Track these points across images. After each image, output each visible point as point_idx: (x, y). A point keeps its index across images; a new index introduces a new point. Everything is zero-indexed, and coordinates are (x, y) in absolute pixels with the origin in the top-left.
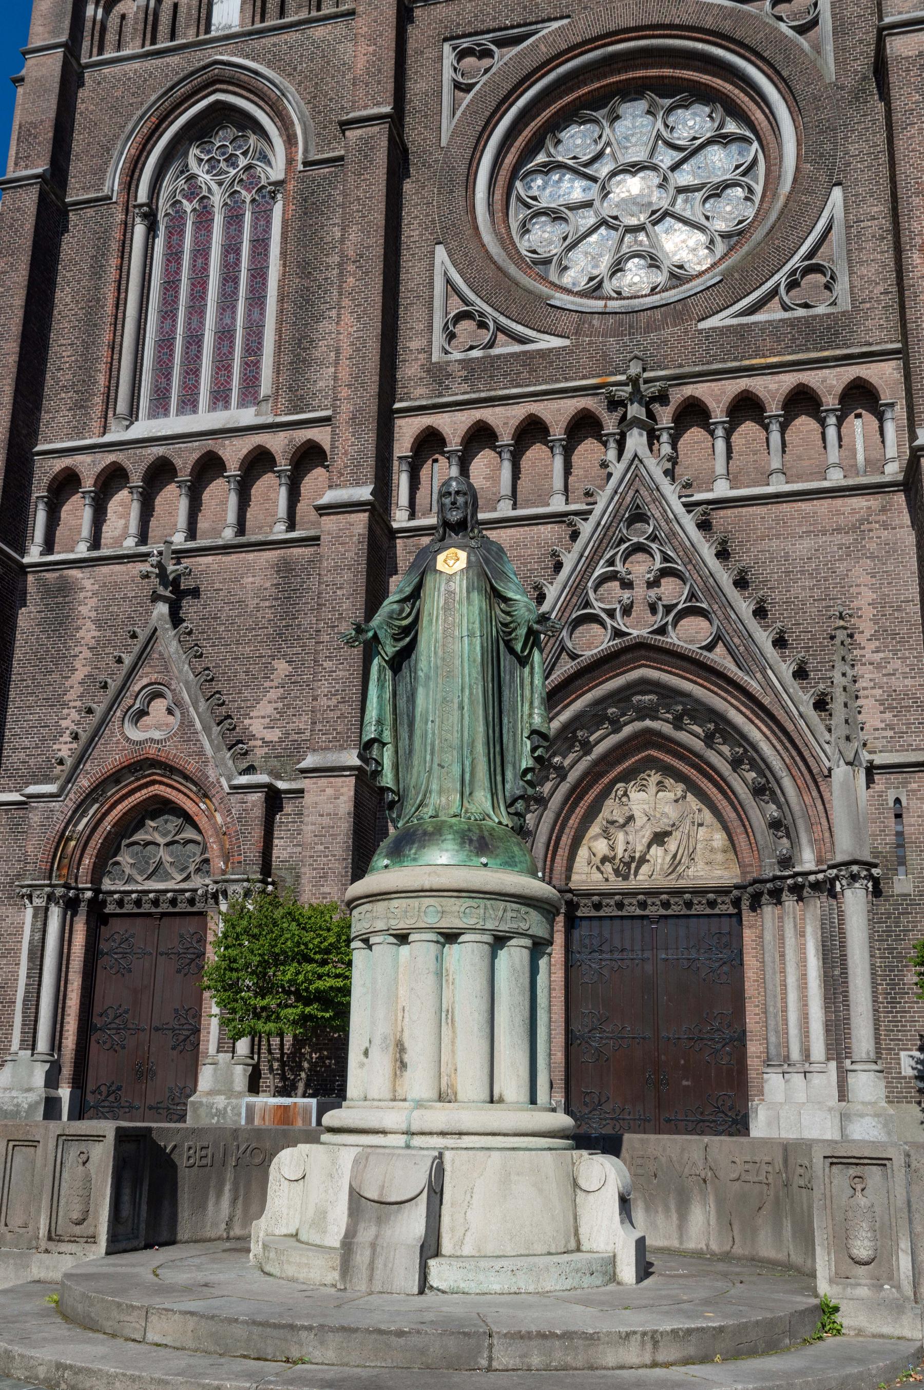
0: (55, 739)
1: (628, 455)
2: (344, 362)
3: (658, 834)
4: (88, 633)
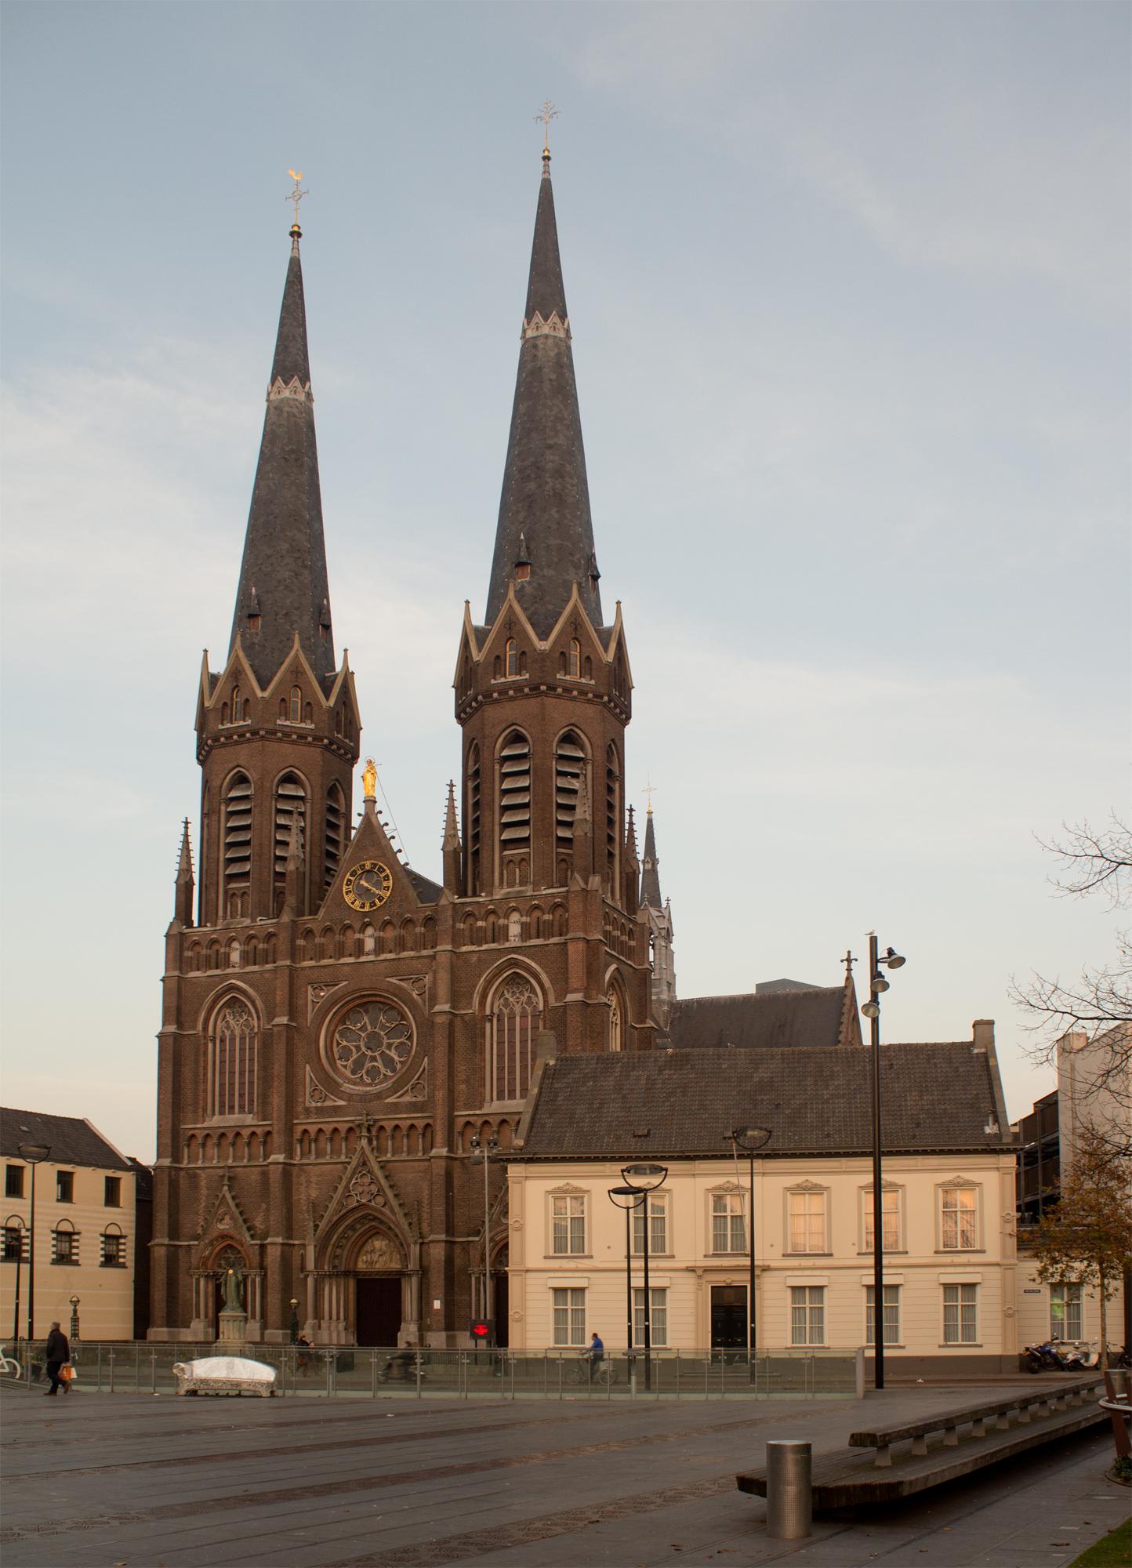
3: (378, 1257)
4: (204, 1191)
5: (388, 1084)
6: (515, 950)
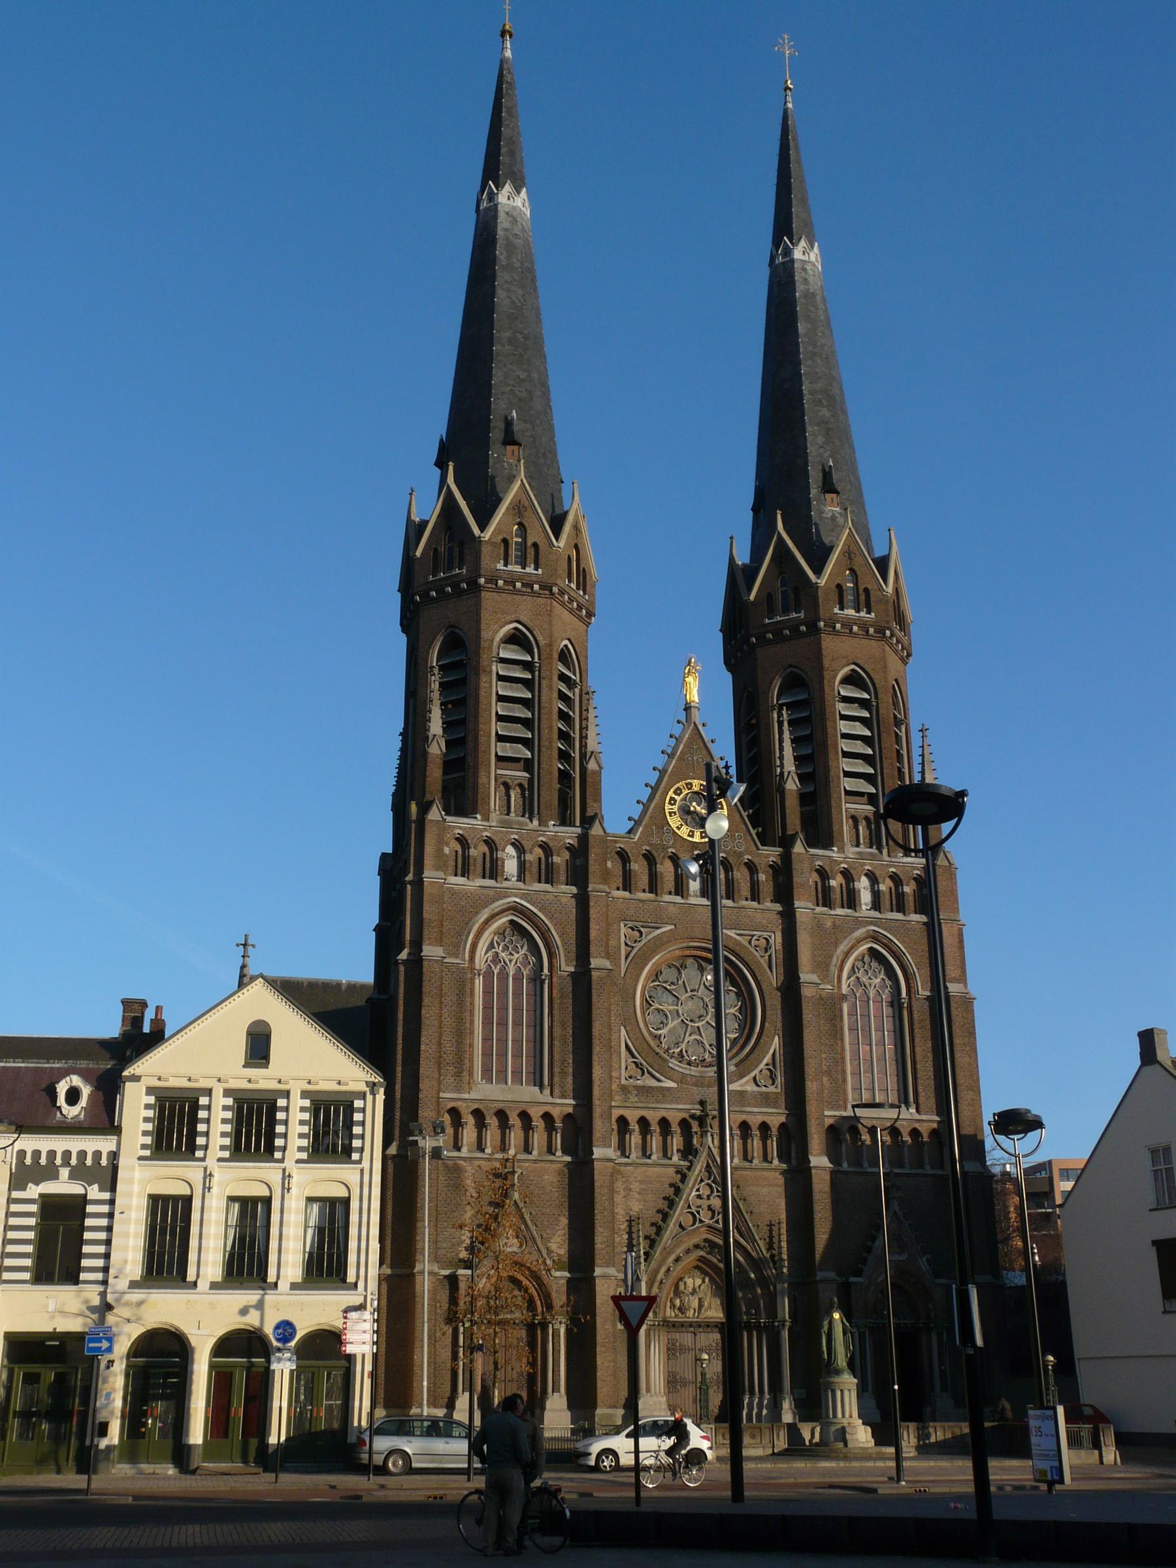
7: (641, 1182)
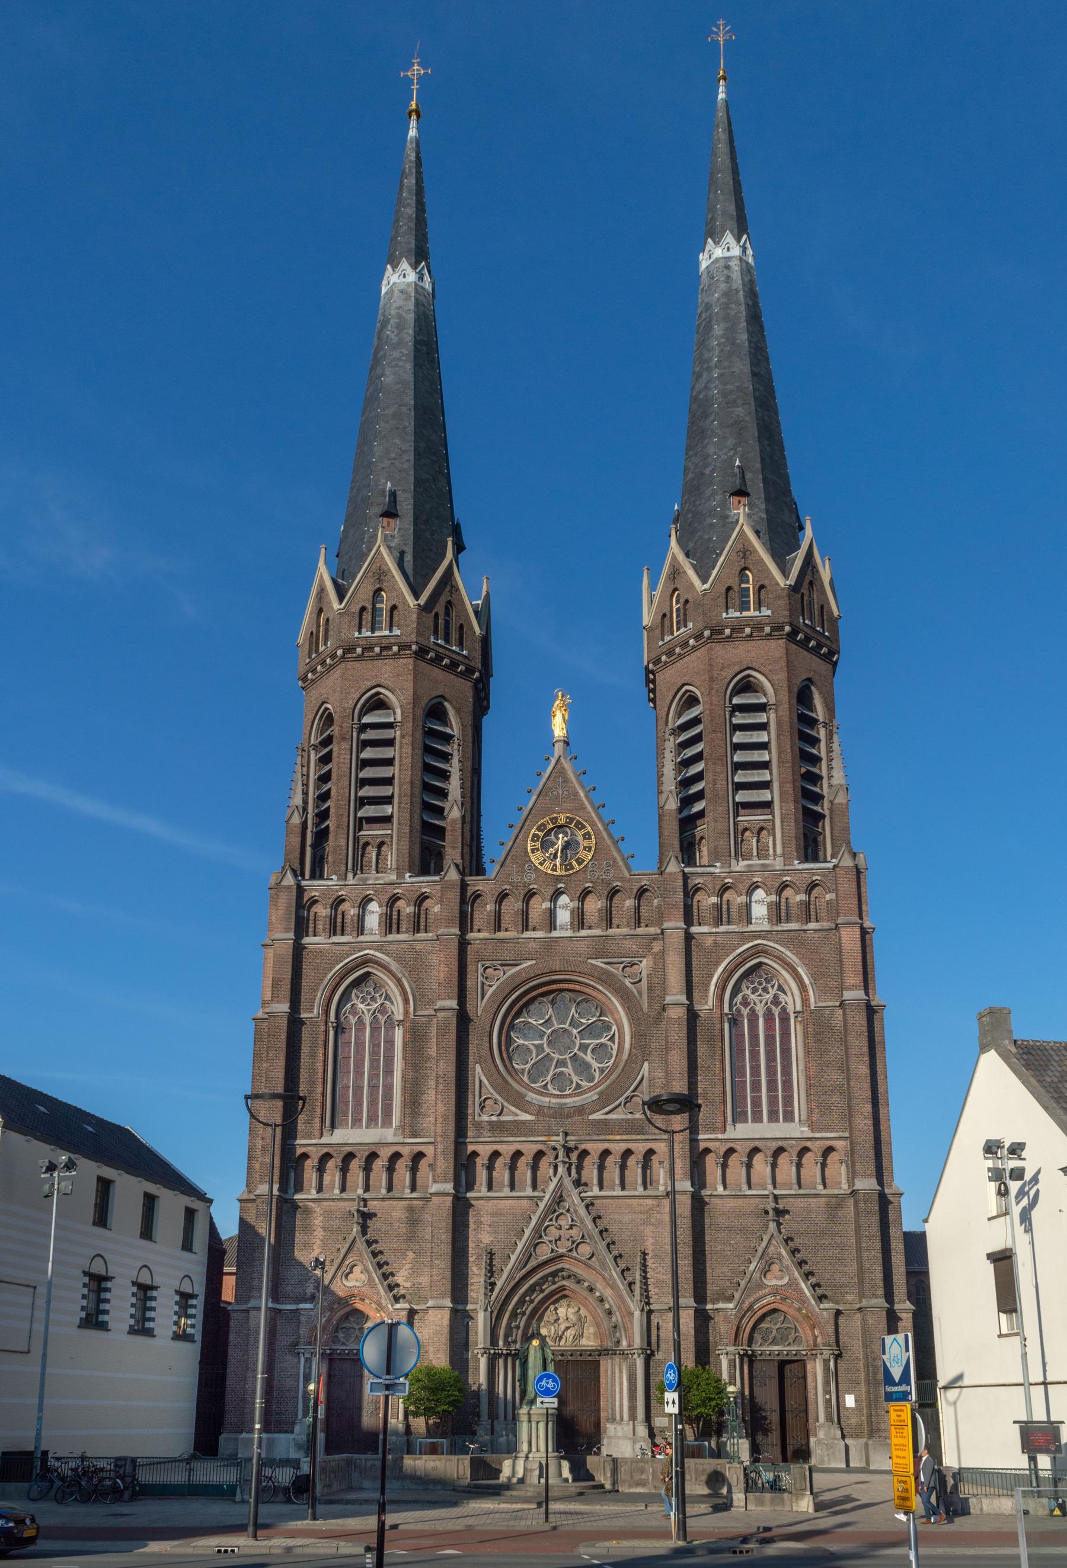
0: (306, 1281)
1: (558, 1176)
2: (439, 1125)
5: (593, 1096)
6: (760, 935)
7: (492, 1215)
